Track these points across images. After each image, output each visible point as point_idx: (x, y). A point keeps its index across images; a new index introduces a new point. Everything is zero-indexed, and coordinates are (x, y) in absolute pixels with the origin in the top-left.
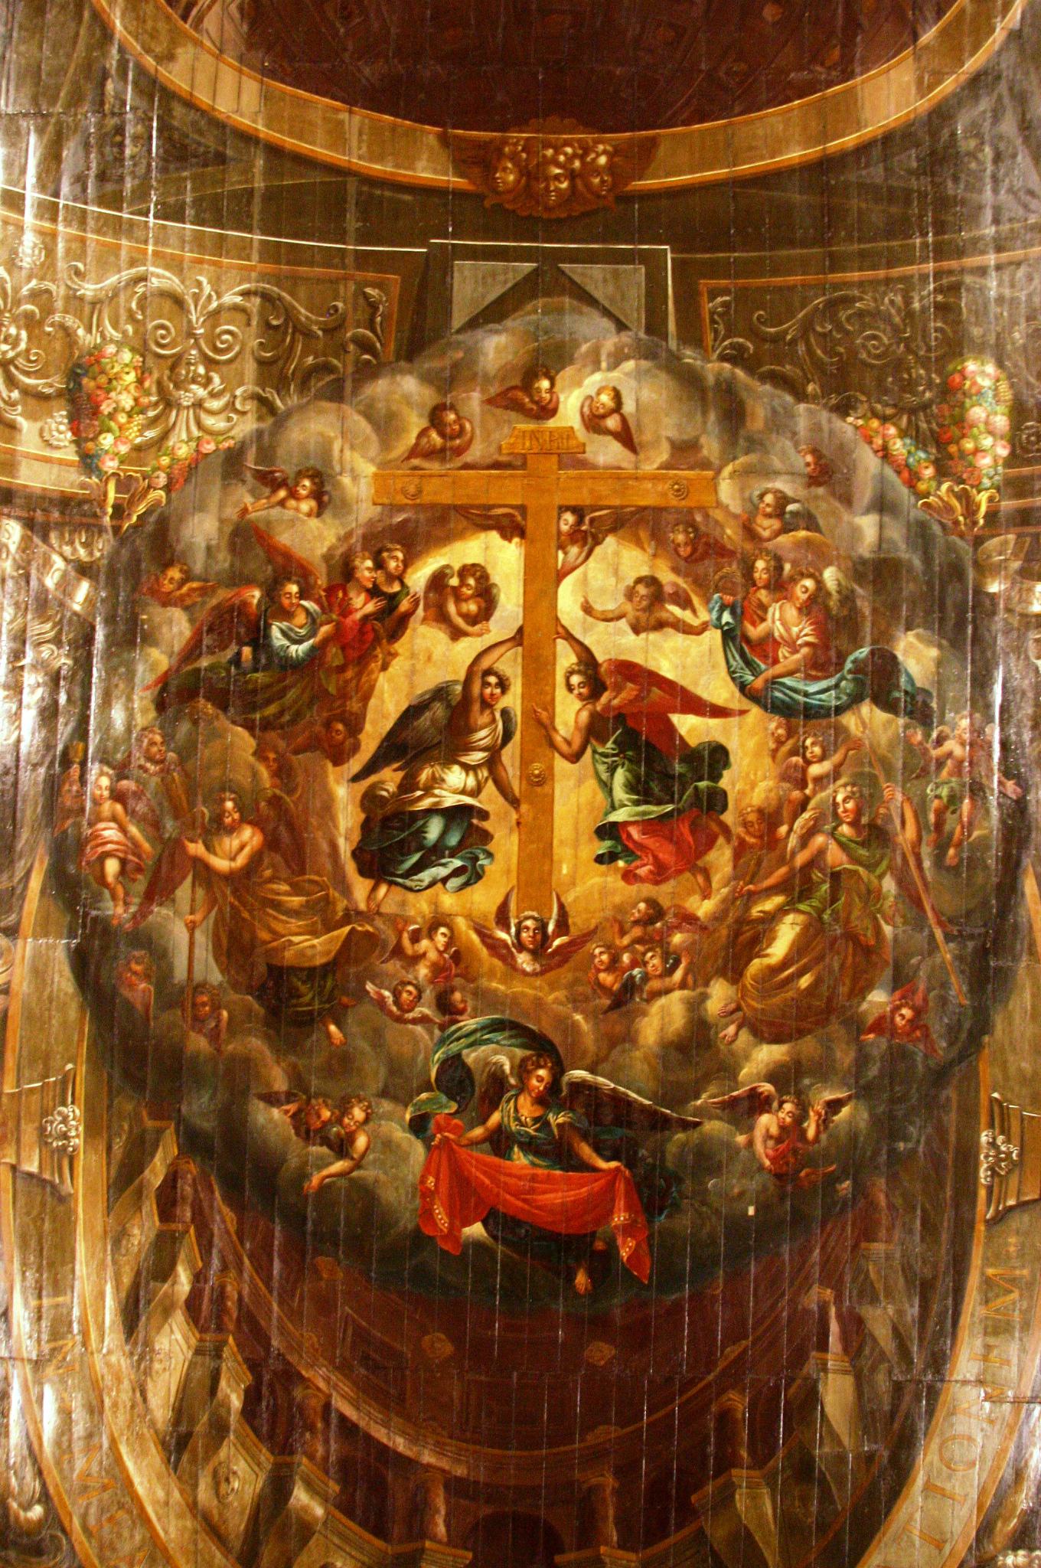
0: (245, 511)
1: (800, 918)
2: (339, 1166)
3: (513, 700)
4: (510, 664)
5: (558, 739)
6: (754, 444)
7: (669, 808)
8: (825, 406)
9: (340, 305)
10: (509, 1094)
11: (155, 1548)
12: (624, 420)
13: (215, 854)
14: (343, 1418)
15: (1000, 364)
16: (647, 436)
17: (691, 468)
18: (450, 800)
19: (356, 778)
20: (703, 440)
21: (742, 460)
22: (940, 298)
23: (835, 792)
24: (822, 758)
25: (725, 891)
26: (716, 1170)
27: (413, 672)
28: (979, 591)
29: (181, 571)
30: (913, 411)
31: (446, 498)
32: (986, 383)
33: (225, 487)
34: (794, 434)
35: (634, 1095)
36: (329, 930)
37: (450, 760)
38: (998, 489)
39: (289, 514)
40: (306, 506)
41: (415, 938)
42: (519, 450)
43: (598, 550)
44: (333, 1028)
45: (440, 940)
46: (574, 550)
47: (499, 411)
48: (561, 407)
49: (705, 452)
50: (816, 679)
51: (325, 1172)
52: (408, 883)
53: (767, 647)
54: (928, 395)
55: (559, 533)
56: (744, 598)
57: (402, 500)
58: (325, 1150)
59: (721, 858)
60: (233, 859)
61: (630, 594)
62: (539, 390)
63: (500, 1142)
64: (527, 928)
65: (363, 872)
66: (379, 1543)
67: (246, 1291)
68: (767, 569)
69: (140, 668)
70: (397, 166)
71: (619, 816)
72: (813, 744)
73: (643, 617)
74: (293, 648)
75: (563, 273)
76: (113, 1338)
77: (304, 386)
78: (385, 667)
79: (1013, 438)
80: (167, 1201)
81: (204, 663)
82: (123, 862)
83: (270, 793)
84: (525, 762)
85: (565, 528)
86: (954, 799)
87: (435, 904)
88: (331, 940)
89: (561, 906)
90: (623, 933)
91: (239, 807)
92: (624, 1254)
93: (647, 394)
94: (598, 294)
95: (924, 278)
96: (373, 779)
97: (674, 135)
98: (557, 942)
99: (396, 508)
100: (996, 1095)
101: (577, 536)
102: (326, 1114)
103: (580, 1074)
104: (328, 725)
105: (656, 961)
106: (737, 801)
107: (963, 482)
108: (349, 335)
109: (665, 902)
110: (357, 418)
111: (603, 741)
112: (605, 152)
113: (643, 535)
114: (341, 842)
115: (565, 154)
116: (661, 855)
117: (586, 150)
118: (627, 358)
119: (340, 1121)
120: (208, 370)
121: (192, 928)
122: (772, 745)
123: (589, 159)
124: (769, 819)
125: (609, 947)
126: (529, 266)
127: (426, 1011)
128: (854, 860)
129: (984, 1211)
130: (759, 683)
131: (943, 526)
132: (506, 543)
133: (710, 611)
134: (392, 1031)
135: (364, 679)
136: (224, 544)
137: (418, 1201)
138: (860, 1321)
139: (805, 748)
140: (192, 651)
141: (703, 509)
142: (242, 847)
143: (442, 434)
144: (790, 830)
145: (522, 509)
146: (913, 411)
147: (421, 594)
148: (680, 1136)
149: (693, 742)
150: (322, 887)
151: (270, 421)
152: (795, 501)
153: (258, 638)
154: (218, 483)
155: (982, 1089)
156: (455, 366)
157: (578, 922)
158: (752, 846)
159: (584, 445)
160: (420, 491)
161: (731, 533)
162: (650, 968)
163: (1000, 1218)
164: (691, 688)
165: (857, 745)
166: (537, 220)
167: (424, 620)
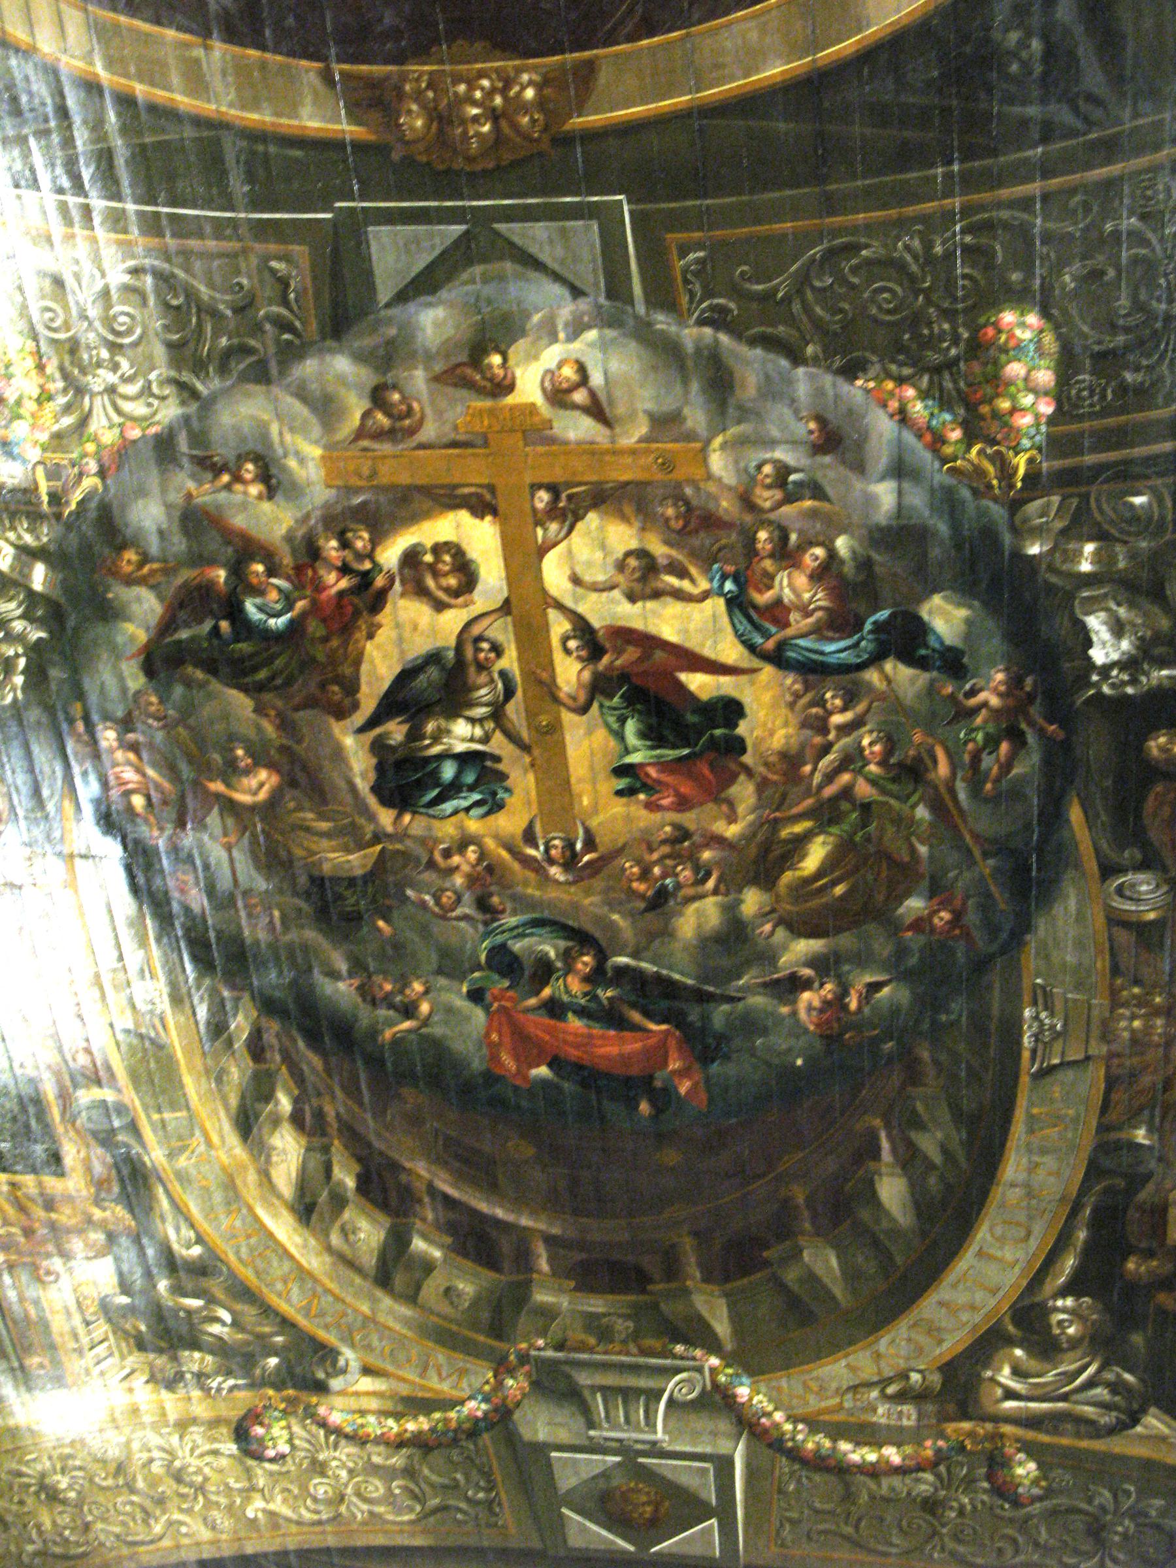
0: (189, 496)
1: (831, 839)
2: (407, 1025)
3: (510, 661)
4: (501, 631)
5: (562, 695)
6: (745, 413)
7: (686, 751)
8: (828, 368)
9: (245, 281)
10: (555, 976)
11: (303, 1274)
12: (592, 394)
13: (237, 790)
14: (446, 1198)
15: (1045, 313)
16: (621, 410)
17: (676, 441)
18: (460, 747)
19: (362, 730)
20: (686, 411)
21: (734, 430)
22: (968, 239)
23: (862, 737)
24: (844, 710)
25: (751, 817)
26: (765, 1032)
27: (400, 640)
28: (1018, 556)
29: (137, 553)
30: (937, 370)
31: (405, 479)
32: (1024, 335)
33: (163, 472)
34: (793, 401)
35: (677, 977)
36: (360, 849)
37: (453, 713)
38: (1040, 449)
39: (238, 498)
40: (254, 490)
41: (447, 854)
42: (477, 428)
43: (580, 526)
44: (381, 923)
45: (472, 853)
46: (553, 527)
47: (450, 390)
48: (519, 382)
49: (689, 424)
50: (831, 640)
51: (396, 1029)
52: (431, 811)
53: (777, 612)
54: (953, 352)
55: (534, 510)
56: (747, 568)
57: (355, 481)
58: (391, 1013)
59: (744, 792)
60: (255, 793)
61: (621, 566)
62: (490, 367)
63: (555, 1008)
64: (556, 847)
65: (386, 802)
66: (494, 1275)
67: (342, 1110)
68: (770, 540)
69: (120, 639)
70: (278, 114)
71: (635, 758)
72: (833, 697)
73: (637, 587)
74: (272, 622)
75: (498, 234)
76: (233, 1138)
77: (223, 370)
78: (371, 636)
79: (1061, 394)
80: (256, 1048)
81: (184, 634)
82: (148, 798)
83: (277, 743)
84: (531, 715)
85: (540, 505)
86: (992, 743)
87: (461, 828)
88: (365, 856)
89: (587, 831)
90: (651, 850)
91: (250, 752)
92: (683, 1090)
93: (615, 365)
94: (544, 257)
95: (948, 217)
96: (378, 731)
97: (617, 55)
98: (586, 858)
99: (350, 490)
100: (1039, 981)
101: (553, 512)
102: (388, 987)
103: (623, 960)
104: (323, 686)
105: (687, 873)
106: (755, 745)
107: (998, 443)
108: (262, 313)
109: (692, 827)
110: (289, 399)
111: (611, 696)
112: (531, 83)
113: (628, 510)
114: (358, 781)
115: (482, 89)
116: (682, 790)
117: (508, 83)
118: (589, 327)
119: (402, 992)
120: (113, 355)
121: (229, 848)
122: (789, 698)
123: (512, 93)
124: (790, 761)
125: (638, 862)
126: (458, 229)
127: (467, 911)
128: (883, 791)
129: (1028, 1066)
130: (770, 644)
131: (975, 492)
132: (477, 521)
133: (711, 580)
134: (438, 928)
135: (350, 648)
136: (175, 528)
137: (485, 1051)
138: (910, 1145)
139: (826, 701)
140: (168, 625)
141: (694, 483)
142: (261, 785)
143: (388, 414)
144: (814, 769)
145: (491, 488)
146: (937, 370)
147: (395, 570)
148: (725, 1007)
149: (704, 696)
150: (347, 815)
151: (193, 407)
152: (796, 470)
153: (234, 612)
154: (154, 472)
155: (1025, 975)
156: (390, 343)
157: (605, 841)
158: (775, 783)
159: (550, 421)
160: (374, 474)
161: (726, 505)
162: (681, 878)
163: (1047, 1072)
164: (697, 650)
165: (882, 697)
166: (458, 173)
167: (403, 595)
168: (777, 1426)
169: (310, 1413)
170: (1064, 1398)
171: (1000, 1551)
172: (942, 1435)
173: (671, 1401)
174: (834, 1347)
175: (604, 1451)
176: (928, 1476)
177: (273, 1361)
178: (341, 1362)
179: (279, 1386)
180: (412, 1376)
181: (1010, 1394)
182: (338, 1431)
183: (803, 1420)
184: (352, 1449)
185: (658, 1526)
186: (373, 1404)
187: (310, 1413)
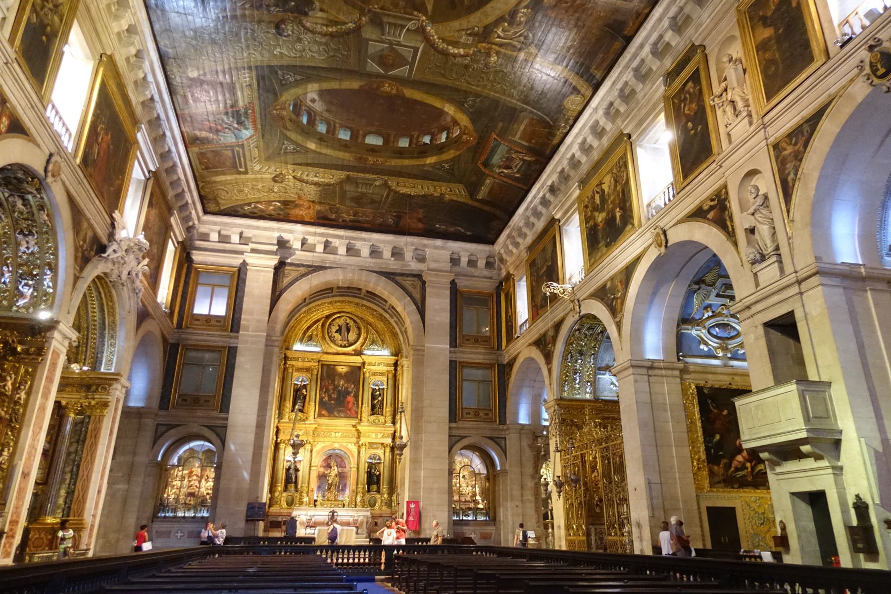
168: (435, 39)
169: (300, 23)
170: (511, 39)
171: (479, 81)
172: (476, 47)
173: (408, 29)
174: (458, 17)
175: (384, 43)
176: (469, 58)
177: (293, 3)
178: (314, 6)
179: (292, 13)
180: (334, 13)
181: (499, 37)
182: (308, 29)
183: (442, 39)
184: (310, 35)
185: (394, 66)
186: (320, 21)
187: (300, 23)
